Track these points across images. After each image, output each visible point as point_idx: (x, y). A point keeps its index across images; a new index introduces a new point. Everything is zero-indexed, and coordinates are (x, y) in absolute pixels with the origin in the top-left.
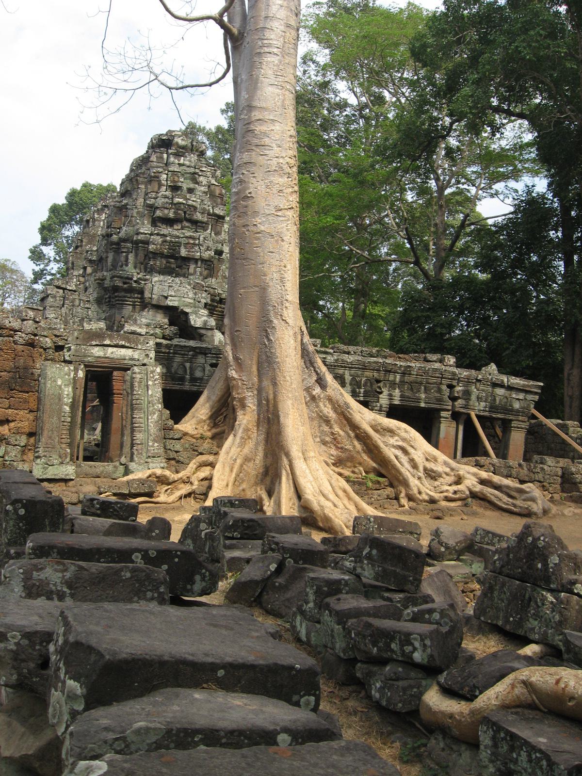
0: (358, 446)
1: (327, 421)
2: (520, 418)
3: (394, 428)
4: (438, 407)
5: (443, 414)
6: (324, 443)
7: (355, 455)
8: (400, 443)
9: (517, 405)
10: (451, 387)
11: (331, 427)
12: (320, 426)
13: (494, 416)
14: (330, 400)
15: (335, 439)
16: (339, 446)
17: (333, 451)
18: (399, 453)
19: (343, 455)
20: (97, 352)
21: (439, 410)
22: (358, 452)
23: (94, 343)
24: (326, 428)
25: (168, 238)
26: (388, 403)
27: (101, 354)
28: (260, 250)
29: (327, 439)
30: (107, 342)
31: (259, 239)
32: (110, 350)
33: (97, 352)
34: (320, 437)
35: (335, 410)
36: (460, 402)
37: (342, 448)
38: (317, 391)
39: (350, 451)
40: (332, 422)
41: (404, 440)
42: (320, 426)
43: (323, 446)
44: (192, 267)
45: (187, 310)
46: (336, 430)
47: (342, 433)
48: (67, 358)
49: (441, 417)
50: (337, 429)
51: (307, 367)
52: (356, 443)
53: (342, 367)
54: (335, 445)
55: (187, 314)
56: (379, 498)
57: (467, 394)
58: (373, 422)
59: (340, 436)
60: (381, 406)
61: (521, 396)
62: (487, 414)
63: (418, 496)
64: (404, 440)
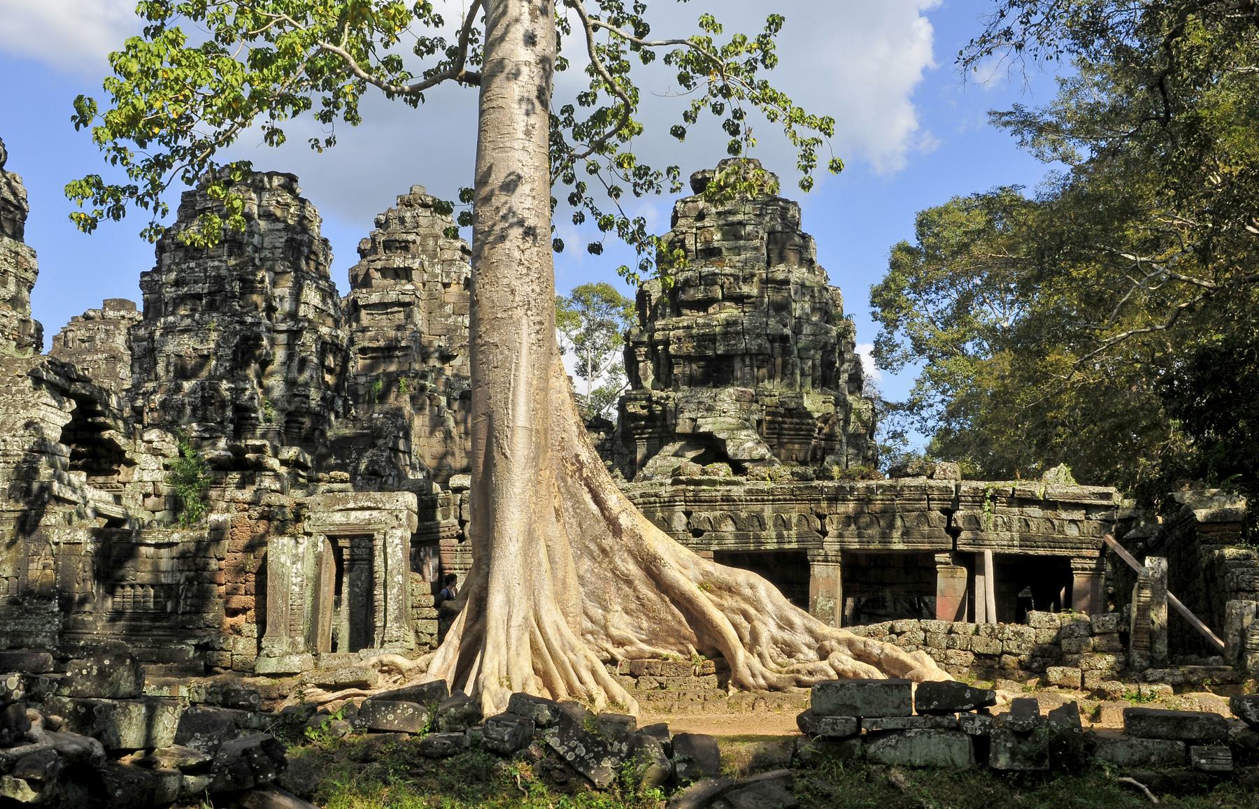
2: (1085, 553)
4: (927, 547)
5: (939, 557)
9: (1072, 532)
10: (948, 513)
12: (619, 589)
13: (1031, 553)
15: (642, 605)
18: (740, 619)
20: (338, 518)
21: (930, 555)
23: (337, 507)
25: (694, 331)
26: (837, 547)
27: (344, 520)
28: (485, 367)
29: (633, 606)
30: (351, 505)
31: (483, 352)
32: (353, 514)
33: (338, 518)
35: (637, 562)
36: (964, 535)
38: (609, 541)
40: (637, 582)
41: (746, 599)
44: (737, 365)
45: (722, 436)
48: (308, 530)
49: (936, 563)
53: (757, 500)
55: (723, 441)
57: (975, 522)
60: (826, 555)
61: (1079, 515)
62: (1016, 550)
64: (746, 599)
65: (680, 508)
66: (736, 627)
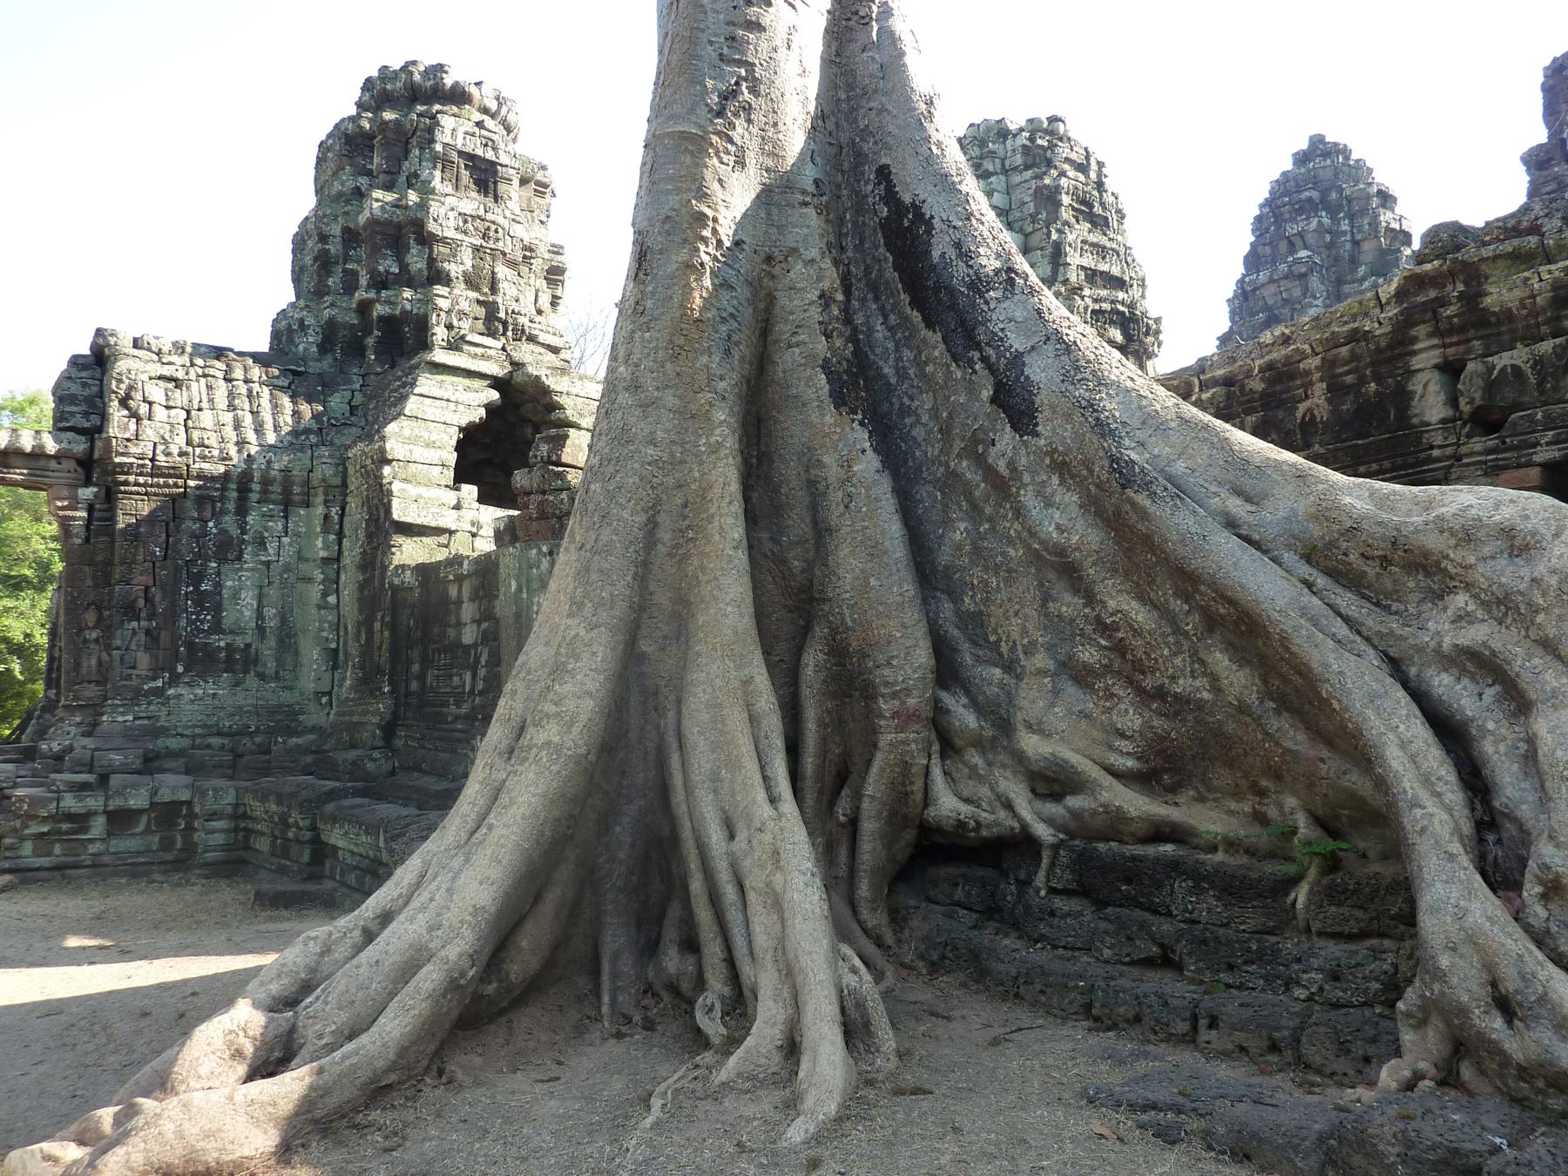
0: (1238, 681)
1: (1070, 572)
3: (1435, 543)
6: (1083, 677)
7: (1230, 727)
8: (1477, 634)
11: (1090, 599)
12: (1046, 599)
14: (1061, 467)
15: (1120, 648)
16: (1148, 683)
17: (1130, 718)
19: (1178, 732)
22: (1243, 709)
24: (1068, 605)
29: (1088, 655)
34: (1050, 649)
37: (1160, 694)
39: (1200, 705)
42: (1046, 599)
43: (1071, 690)
46: (1112, 604)
47: (1140, 615)
50: (1120, 601)
51: (955, 358)
52: (1220, 660)
54: (1130, 682)
56: (1335, 993)
58: (1316, 531)
59: (1137, 633)
63: (1495, 1025)
64: (1502, 605)
65: (1426, 356)
66: (1450, 732)
